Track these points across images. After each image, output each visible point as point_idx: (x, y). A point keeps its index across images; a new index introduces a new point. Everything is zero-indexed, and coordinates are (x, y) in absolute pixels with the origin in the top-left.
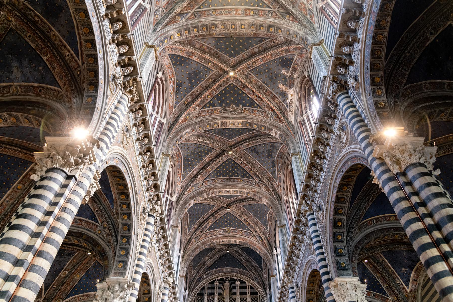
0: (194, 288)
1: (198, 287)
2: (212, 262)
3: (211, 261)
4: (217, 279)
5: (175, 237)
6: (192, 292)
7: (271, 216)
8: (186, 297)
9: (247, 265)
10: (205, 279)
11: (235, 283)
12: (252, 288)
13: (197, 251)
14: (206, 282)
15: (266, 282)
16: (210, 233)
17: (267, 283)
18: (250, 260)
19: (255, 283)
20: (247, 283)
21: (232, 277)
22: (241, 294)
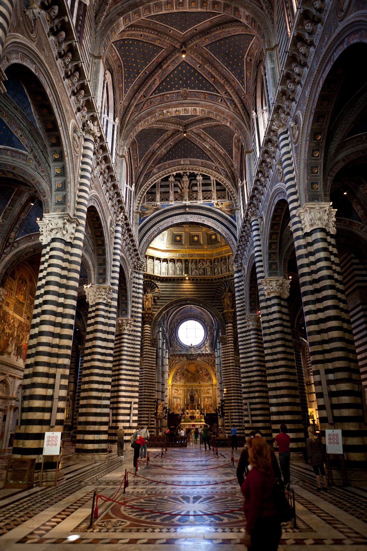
0: (142, 186)
1: (147, 184)
2: (163, 151)
5: (97, 72)
6: (139, 190)
7: (251, 60)
8: (133, 193)
10: (156, 174)
11: (195, 179)
12: (218, 184)
13: (140, 124)
14: (157, 178)
15: (237, 173)
16: (158, 98)
18: (216, 146)
19: (223, 178)
20: (212, 178)
21: (192, 171)
22: (203, 191)
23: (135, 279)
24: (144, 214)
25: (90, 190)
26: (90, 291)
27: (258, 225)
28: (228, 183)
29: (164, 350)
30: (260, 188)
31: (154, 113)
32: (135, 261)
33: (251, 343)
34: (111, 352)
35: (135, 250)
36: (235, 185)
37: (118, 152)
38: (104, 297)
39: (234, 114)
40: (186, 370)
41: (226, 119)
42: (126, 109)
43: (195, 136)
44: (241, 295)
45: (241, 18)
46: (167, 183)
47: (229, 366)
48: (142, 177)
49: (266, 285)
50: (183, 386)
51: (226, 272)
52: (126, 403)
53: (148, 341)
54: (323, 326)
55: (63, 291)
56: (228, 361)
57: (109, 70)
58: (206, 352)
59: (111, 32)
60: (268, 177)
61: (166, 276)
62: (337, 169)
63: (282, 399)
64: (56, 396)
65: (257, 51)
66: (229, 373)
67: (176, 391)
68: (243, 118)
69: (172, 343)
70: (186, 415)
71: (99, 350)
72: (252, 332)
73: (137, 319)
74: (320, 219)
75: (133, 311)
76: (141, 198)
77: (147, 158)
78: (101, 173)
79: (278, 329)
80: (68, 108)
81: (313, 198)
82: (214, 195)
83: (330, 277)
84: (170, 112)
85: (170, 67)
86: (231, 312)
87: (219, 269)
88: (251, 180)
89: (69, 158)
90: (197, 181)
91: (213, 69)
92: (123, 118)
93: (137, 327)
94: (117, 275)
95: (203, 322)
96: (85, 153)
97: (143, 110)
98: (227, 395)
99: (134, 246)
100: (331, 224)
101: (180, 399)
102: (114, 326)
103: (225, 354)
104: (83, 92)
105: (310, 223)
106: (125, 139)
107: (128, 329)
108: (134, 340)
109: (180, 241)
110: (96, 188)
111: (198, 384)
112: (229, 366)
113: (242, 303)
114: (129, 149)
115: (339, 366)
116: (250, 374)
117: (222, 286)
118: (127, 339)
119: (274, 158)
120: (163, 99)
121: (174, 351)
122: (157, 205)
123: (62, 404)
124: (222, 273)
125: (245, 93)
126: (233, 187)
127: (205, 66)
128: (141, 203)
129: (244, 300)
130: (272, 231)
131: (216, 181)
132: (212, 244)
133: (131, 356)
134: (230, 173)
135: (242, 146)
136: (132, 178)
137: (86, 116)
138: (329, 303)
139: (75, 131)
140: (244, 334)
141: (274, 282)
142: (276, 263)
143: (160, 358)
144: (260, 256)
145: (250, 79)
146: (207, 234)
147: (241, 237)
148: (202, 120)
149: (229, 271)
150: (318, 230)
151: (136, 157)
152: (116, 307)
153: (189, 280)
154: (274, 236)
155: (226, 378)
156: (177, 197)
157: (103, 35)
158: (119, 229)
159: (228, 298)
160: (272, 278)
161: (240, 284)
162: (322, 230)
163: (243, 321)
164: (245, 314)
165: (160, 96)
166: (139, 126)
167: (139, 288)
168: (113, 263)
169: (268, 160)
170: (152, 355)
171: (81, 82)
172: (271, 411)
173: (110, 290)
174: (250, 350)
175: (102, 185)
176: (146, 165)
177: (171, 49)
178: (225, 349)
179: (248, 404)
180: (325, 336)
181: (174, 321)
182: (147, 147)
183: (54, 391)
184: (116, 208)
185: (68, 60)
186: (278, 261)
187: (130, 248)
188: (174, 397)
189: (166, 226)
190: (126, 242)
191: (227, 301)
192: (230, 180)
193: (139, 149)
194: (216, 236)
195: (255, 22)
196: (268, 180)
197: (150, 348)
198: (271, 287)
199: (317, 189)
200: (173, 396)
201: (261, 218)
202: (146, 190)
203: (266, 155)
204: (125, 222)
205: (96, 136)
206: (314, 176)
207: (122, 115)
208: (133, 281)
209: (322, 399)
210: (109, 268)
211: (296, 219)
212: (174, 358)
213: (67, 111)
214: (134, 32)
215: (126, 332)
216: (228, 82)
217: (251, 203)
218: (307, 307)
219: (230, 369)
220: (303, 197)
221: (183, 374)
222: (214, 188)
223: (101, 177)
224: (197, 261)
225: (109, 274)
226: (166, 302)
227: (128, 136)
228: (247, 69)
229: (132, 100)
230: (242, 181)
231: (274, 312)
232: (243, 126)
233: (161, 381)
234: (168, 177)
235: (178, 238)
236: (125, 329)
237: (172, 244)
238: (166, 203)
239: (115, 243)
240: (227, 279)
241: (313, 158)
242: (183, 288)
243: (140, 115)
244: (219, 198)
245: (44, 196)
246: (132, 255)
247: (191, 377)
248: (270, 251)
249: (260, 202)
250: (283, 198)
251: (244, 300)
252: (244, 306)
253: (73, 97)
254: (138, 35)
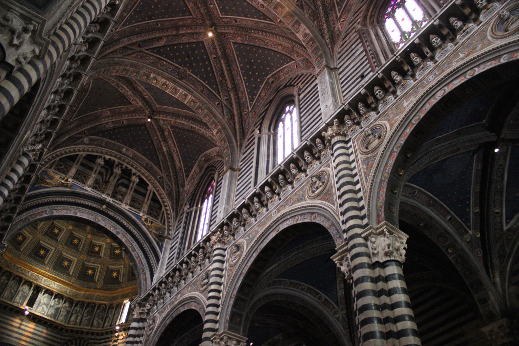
6: (53, 150)
10: (85, 144)
14: (84, 151)
20: (150, 187)
36: (177, 209)
39: (226, 124)
45: (298, 33)
51: (87, 325)
84: (157, 80)
87: (79, 318)
90: (130, 181)
126: (173, 210)
134: (176, 192)
146: (84, 264)
149: (91, 326)
151: (74, 108)
166: (114, 69)
230: (191, 206)
238: (80, 184)
240: (84, 336)
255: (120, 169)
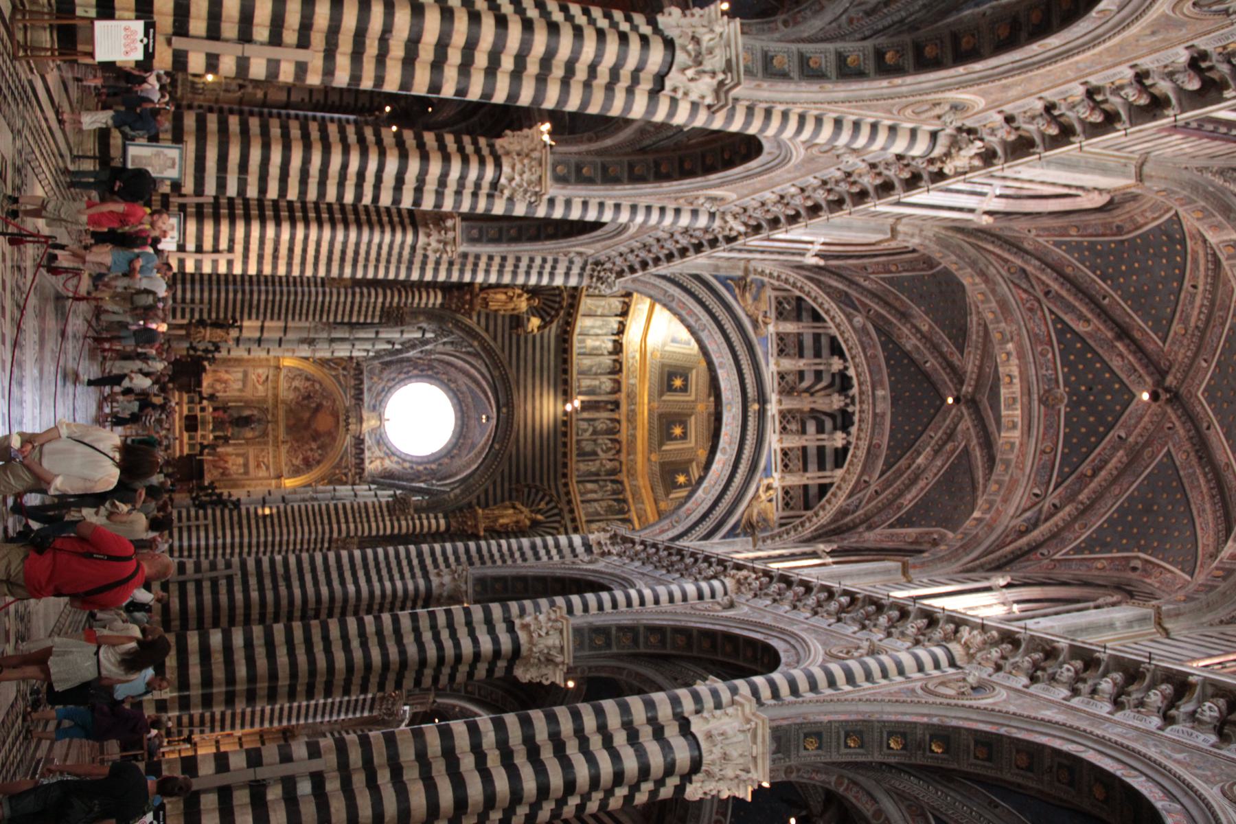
0: (818, 283)
1: (823, 298)
2: (910, 342)
3: (914, 341)
4: (850, 364)
5: (1104, 170)
7: (1134, 569)
9: (900, 473)
10: (850, 321)
11: (835, 428)
12: (823, 489)
13: (977, 280)
14: (838, 326)
15: (851, 541)
16: (1043, 328)
17: (846, 543)
18: (921, 483)
20: (839, 473)
21: (856, 418)
22: (804, 449)
23: (566, 264)
24: (744, 289)
25: (804, 143)
26: (532, 141)
27: (713, 596)
28: (825, 515)
29: (374, 345)
30: (811, 600)
31: (1005, 319)
32: (614, 264)
33: (392, 579)
34: (367, 199)
35: (644, 265)
36: (820, 536)
37: (904, 221)
38: (517, 178)
40: (319, 407)
41: (989, 509)
42: (1014, 245)
43: (948, 427)
44: (523, 554)
46: (825, 351)
47: (330, 523)
48: (840, 286)
49: (549, 619)
50: (276, 396)
51: (587, 514)
52: (232, 241)
53: (396, 299)
54: (439, 768)
55: (533, 68)
56: (343, 520)
57: (1111, 202)
58: (367, 462)
59: (1203, 210)
60: (839, 620)
61: (575, 350)
62: (856, 797)
63: (243, 662)
64: (249, 49)
65: (1157, 585)
66: (312, 522)
67: (264, 377)
68: (992, 552)
69: (393, 368)
70: (198, 407)
71: (372, 166)
72: (421, 583)
73: (456, 268)
74: (725, 757)
75: (477, 257)
76: (786, 281)
77: (891, 299)
78: (849, 175)
79: (432, 652)
80: (1013, 93)
81: (782, 739)
82: (794, 480)
83: (570, 786)
84: (1008, 360)
85: (1120, 360)
86: (476, 526)
87: (594, 496)
88: (831, 577)
89: (885, 91)
91: (1115, 473)
92: (993, 235)
93: (436, 270)
94: (575, 214)
95: (449, 452)
96: (900, 133)
97: (1014, 290)
98: (252, 516)
99: (657, 261)
100: (711, 787)
101: (241, 390)
102: (438, 205)
103: (363, 511)
104: (1053, 131)
105: (715, 732)
106: (940, 241)
107: (429, 244)
108: (399, 261)
109: (670, 388)
110: (810, 160)
111: (281, 438)
112: (330, 523)
113: (502, 556)
114: (914, 251)
115: (333, 810)
116: (308, 577)
117: (547, 504)
118: (403, 243)
119: (889, 635)
120: (1041, 343)
121: (371, 372)
122: (766, 324)
123: (228, 65)
124: (583, 502)
125: (1057, 557)
126: (816, 530)
127: (1121, 453)
128: (772, 281)
129: (509, 562)
130: (695, 633)
131: (831, 484)
132: (662, 476)
133: (356, 253)
134: (852, 520)
135: (921, 552)
136: (837, 257)
137: (993, 139)
138: (502, 784)
139: (955, 108)
140: (415, 562)
141: (557, 642)
142: (609, 645)
143: (351, 333)
144: (629, 603)
145: (1089, 568)
146: (690, 461)
147: (680, 552)
148: (988, 443)
150: (696, 753)
151: (893, 268)
152: (488, 210)
153: (565, 413)
154: (681, 640)
155: (297, 514)
156: (790, 378)
157: (1195, 187)
158: (703, 221)
159: (514, 519)
160: (569, 636)
161: (554, 552)
162: (696, 765)
163: (452, 559)
164: (471, 563)
165: (1049, 335)
166: (972, 276)
167: (540, 274)
168: (610, 203)
169: (883, 620)
170: (359, 312)
171: (1078, 128)
172: (212, 631)
173: (536, 193)
174: (375, 578)
175: (817, 175)
176: (873, 295)
177: (1163, 364)
178: (375, 512)
179: (229, 572)
180: (411, 774)
181: (454, 373)
182: (920, 299)
183: (262, 44)
184: (759, 214)
185: (1132, 94)
186: (615, 650)
187: (649, 251)
188: (246, 374)
189: (711, 348)
190: (665, 240)
191: (507, 517)
192: (834, 521)
193: (913, 278)
194: (686, 486)
195: (1224, 578)
196: (832, 620)
197: (379, 305)
198: (543, 633)
199: (805, 749)
200: (250, 370)
201: (731, 605)
202: (808, 294)
203: (895, 614)
204: (720, 237)
205: (943, 162)
206: (839, 738)
207: (1000, 233)
208: (561, 257)
209: (245, 764)
210: (596, 193)
211: (725, 696)
212: (352, 372)
213: (1006, 88)
214: (1202, 268)
215: (422, 239)
216: (1082, 513)
217: (771, 578)
218: (490, 726)
219: (322, 523)
220: (786, 712)
221: (308, 397)
222: (813, 478)
223: (838, 174)
224: (615, 433)
225: (578, 193)
226: (503, 350)
227: (947, 247)
228: (1112, 559)
229: (1038, 259)
230: (832, 553)
231: (475, 641)
232: (971, 552)
233: (290, 336)
234: (842, 355)
235: (678, 383)
236: (428, 235)
237: (663, 365)
238: (773, 348)
239: (662, 210)
240: (568, 517)
241: (885, 735)
242: (541, 395)
243: (1001, 281)
244: (786, 492)
245: (786, 23)
246: (631, 257)
247: (301, 420)
248: (641, 630)
249: (775, 601)
250: (783, 660)
251: (509, 562)
252: (494, 562)
253: (1039, 106)
254: (1195, 278)
255: (842, 404)
